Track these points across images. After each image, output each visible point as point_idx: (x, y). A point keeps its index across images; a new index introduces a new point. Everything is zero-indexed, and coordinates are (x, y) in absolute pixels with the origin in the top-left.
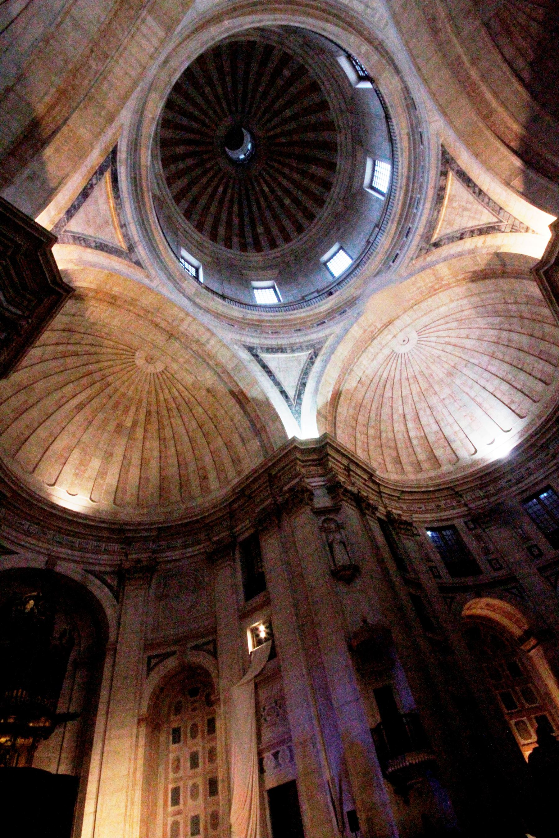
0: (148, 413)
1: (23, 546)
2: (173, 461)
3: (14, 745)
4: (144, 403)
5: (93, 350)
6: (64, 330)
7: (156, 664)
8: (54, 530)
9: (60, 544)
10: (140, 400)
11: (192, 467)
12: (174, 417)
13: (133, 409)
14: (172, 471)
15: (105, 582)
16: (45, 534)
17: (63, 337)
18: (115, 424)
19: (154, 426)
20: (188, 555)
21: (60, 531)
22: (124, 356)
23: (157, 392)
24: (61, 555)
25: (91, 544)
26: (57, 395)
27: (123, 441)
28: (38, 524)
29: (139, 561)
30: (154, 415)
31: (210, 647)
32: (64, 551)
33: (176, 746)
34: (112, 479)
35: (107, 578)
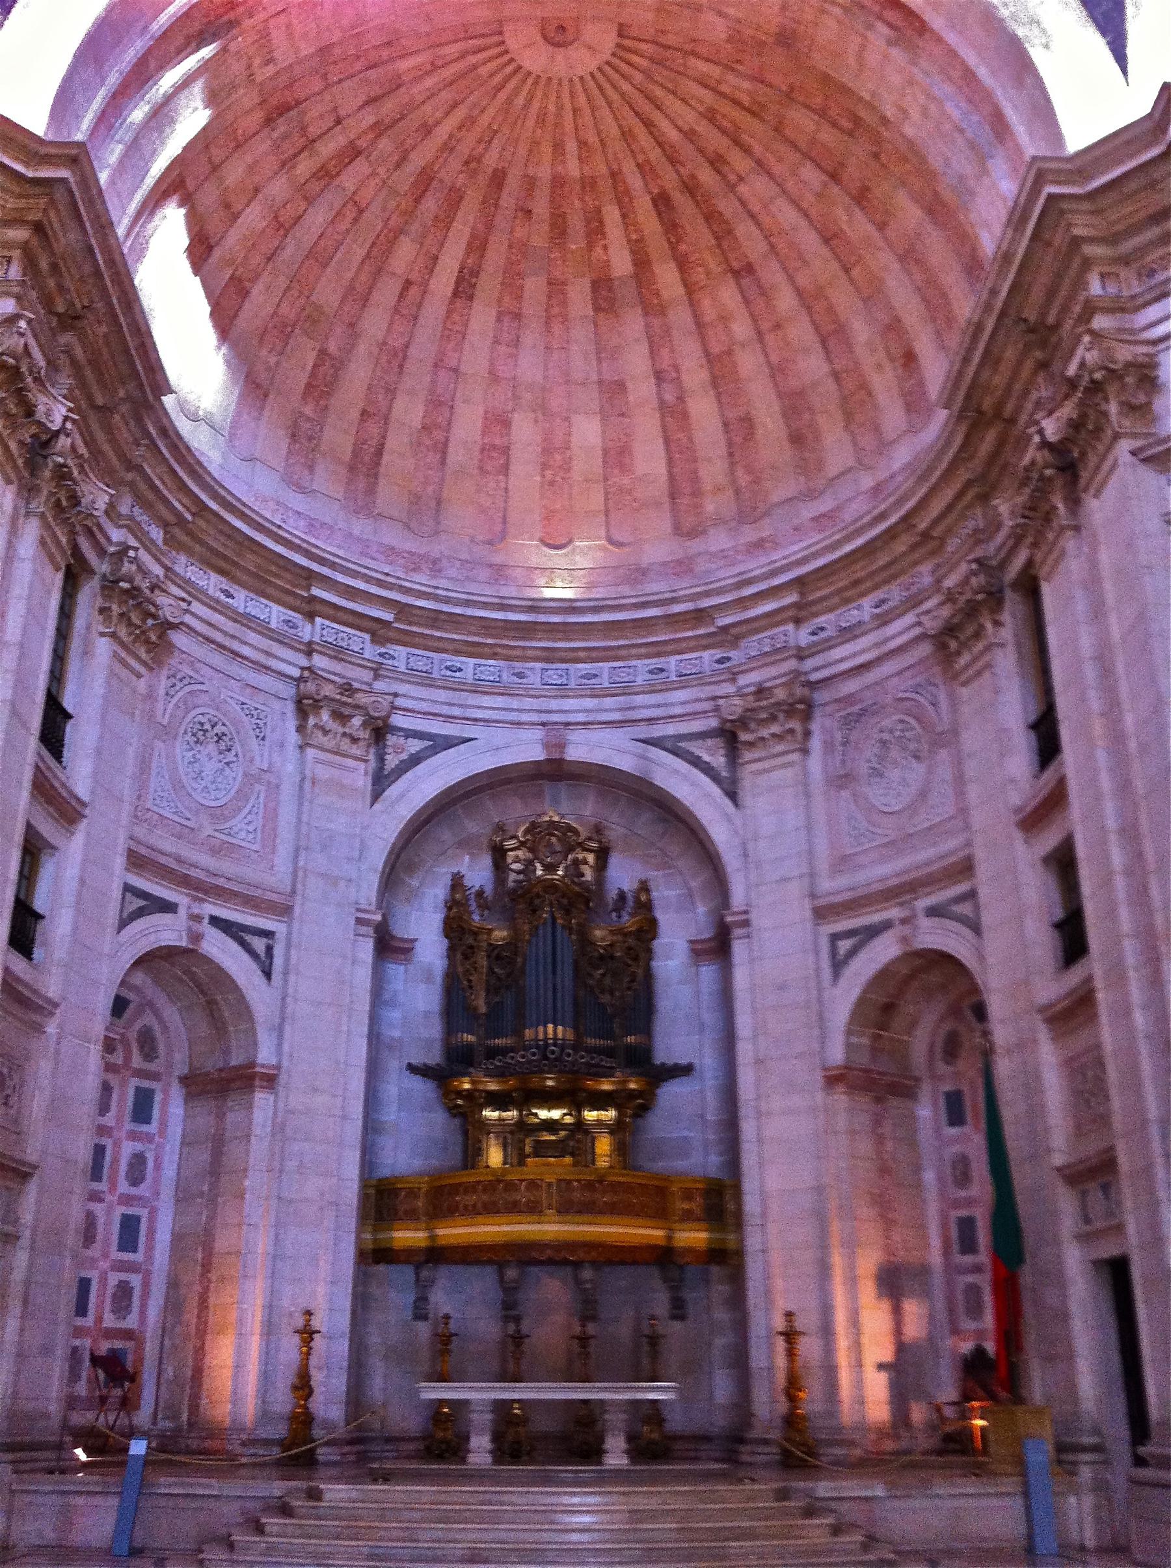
0: (662, 202)
2: (801, 331)
3: (580, 1124)
4: (635, 182)
5: (389, 108)
6: (269, 121)
7: (852, 953)
8: (537, 659)
9: (563, 691)
10: (614, 175)
11: (861, 331)
12: (741, 179)
13: (612, 215)
14: (812, 366)
15: (696, 762)
16: (520, 675)
17: (285, 137)
18: (585, 284)
19: (698, 234)
20: (893, 644)
21: (549, 656)
22: (483, 71)
23: (648, 124)
24: (572, 718)
25: (641, 668)
26: (386, 293)
27: (633, 324)
28: (494, 656)
29: (761, 691)
30: (684, 205)
31: (965, 909)
32: (575, 707)
33: (953, 1131)
34: (650, 459)
35: (700, 750)
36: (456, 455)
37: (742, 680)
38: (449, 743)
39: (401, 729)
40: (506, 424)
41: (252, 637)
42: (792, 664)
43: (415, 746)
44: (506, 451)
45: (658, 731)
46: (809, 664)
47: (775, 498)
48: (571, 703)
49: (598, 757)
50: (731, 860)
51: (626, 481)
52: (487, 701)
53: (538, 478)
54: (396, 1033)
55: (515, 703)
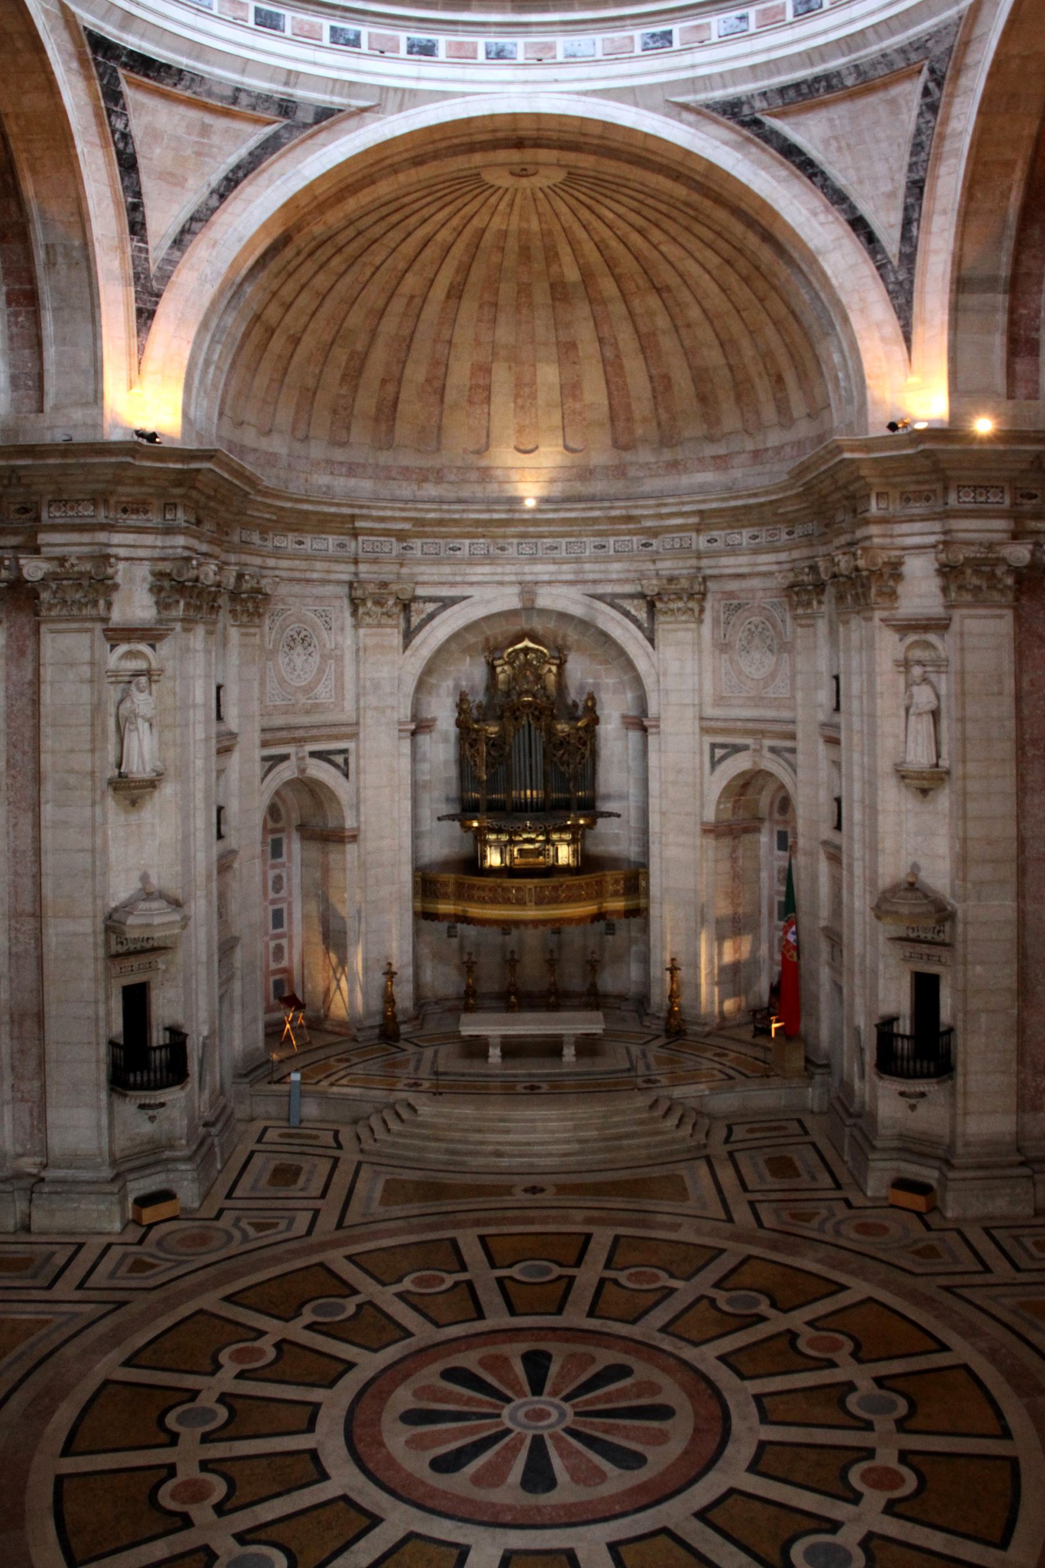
1: (472, 584)
29: (671, 580)
32: (542, 570)
36: (450, 396)
37: (660, 565)
38: (453, 601)
39: (421, 597)
40: (489, 371)
41: (319, 565)
42: (693, 562)
43: (430, 607)
44: (488, 388)
45: (600, 590)
46: (704, 562)
47: (686, 434)
48: (539, 568)
49: (560, 605)
50: (649, 682)
51: (578, 406)
52: (479, 569)
53: (512, 405)
54: (427, 778)
55: (499, 570)
